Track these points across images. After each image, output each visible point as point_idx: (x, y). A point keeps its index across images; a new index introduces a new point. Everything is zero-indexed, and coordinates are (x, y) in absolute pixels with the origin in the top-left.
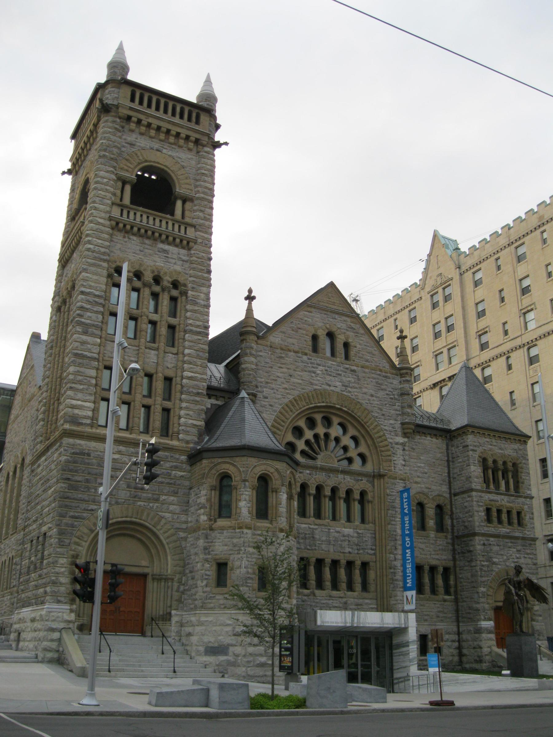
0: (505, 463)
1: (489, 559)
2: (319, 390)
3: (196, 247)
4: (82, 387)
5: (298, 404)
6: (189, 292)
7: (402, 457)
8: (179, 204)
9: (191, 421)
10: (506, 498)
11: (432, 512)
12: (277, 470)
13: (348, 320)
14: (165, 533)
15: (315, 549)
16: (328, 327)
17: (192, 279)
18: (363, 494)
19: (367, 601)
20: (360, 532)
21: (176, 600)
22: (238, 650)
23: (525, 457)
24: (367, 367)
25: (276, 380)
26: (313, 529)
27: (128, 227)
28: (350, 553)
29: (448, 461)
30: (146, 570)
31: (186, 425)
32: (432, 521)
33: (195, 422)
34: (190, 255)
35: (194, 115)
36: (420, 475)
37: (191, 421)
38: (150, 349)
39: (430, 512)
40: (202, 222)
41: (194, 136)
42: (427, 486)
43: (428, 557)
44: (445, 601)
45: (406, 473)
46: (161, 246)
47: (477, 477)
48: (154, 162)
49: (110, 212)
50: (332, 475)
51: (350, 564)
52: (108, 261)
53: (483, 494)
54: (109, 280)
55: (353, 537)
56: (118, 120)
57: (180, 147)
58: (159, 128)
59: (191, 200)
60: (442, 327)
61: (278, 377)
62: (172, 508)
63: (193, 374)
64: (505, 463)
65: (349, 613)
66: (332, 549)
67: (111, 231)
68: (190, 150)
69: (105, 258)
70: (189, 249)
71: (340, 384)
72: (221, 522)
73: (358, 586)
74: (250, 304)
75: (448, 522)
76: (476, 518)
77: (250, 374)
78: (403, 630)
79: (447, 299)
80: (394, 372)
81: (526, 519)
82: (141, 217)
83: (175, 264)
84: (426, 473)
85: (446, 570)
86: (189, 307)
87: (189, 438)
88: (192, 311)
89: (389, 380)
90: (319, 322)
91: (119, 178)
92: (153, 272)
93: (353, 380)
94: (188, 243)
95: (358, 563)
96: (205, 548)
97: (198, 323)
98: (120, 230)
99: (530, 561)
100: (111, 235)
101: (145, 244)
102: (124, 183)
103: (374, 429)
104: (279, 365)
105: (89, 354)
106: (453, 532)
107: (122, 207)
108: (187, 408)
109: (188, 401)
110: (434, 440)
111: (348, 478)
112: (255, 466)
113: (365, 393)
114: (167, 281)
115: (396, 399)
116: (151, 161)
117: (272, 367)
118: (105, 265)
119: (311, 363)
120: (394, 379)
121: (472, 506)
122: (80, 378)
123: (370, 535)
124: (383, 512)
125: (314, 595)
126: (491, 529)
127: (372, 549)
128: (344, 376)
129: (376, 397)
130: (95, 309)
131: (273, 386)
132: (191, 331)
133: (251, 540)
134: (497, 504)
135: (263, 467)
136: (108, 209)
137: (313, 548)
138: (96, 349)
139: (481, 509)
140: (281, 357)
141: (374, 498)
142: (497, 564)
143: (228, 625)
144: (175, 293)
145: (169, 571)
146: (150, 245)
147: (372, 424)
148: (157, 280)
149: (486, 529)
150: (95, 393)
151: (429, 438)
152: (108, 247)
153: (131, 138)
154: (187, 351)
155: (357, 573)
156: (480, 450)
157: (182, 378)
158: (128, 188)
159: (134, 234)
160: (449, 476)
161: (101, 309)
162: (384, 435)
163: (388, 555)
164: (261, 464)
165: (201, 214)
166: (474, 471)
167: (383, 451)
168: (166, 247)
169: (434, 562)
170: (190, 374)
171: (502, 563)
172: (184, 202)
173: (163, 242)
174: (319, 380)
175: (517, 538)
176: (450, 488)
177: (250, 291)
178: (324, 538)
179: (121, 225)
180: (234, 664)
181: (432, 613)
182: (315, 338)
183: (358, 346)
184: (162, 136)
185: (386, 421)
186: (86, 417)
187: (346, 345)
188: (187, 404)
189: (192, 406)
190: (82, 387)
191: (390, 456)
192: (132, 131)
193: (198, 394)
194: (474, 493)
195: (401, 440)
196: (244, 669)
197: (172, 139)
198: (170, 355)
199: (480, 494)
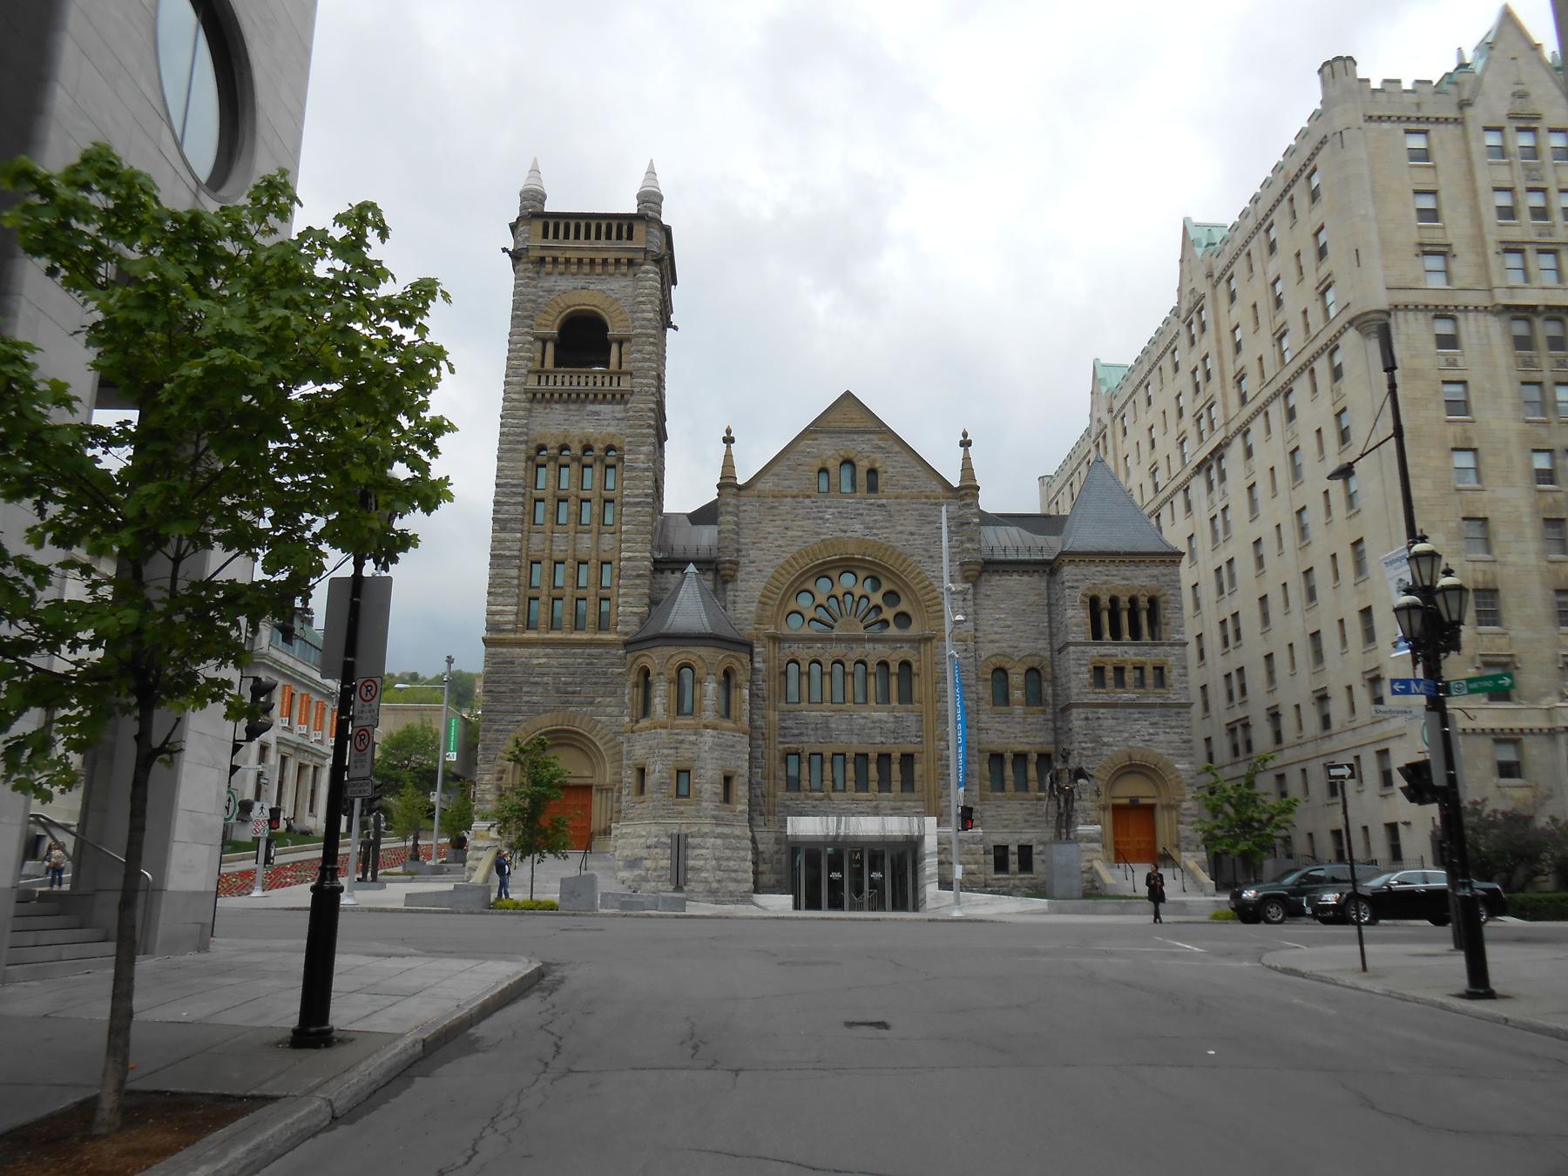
0: (1133, 601)
1: (1096, 740)
10: (1132, 650)
18: (906, 665)
22: (648, 863)
23: (1175, 585)
24: (905, 497)
27: (548, 396)
29: (1049, 605)
30: (589, 781)
34: (626, 411)
35: (625, 228)
39: (1016, 679)
41: (624, 256)
44: (1039, 799)
46: (591, 408)
47: (1077, 625)
51: (884, 758)
52: (526, 442)
53: (1088, 648)
57: (611, 275)
58: (580, 261)
59: (628, 340)
60: (1200, 376)
62: (609, 710)
64: (1133, 601)
65: (833, 820)
66: (855, 740)
68: (625, 275)
72: (644, 723)
73: (896, 786)
74: (729, 447)
75: (1048, 690)
76: (1073, 684)
78: (921, 838)
79: (1203, 328)
81: (1172, 675)
82: (567, 380)
85: (1045, 759)
87: (628, 629)
88: (630, 479)
90: (829, 450)
91: (537, 338)
95: (896, 755)
98: (540, 402)
99: (1176, 738)
100: (530, 410)
102: (544, 342)
105: (507, 553)
106: (1055, 705)
107: (539, 373)
108: (625, 595)
110: (1026, 578)
111: (879, 647)
114: (598, 447)
118: (523, 447)
126: (1102, 696)
138: (517, 546)
148: (587, 448)
151: (1015, 577)
152: (526, 425)
153: (548, 283)
155: (895, 768)
156: (1084, 586)
158: (550, 347)
160: (1050, 627)
165: (638, 356)
168: (596, 408)
169: (1019, 748)
172: (621, 344)
173: (592, 402)
175: (1152, 706)
176: (1051, 644)
179: (539, 396)
180: (645, 879)
184: (586, 269)
186: (507, 623)
187: (872, 472)
192: (549, 274)
193: (639, 576)
194: (1071, 648)
197: (598, 269)
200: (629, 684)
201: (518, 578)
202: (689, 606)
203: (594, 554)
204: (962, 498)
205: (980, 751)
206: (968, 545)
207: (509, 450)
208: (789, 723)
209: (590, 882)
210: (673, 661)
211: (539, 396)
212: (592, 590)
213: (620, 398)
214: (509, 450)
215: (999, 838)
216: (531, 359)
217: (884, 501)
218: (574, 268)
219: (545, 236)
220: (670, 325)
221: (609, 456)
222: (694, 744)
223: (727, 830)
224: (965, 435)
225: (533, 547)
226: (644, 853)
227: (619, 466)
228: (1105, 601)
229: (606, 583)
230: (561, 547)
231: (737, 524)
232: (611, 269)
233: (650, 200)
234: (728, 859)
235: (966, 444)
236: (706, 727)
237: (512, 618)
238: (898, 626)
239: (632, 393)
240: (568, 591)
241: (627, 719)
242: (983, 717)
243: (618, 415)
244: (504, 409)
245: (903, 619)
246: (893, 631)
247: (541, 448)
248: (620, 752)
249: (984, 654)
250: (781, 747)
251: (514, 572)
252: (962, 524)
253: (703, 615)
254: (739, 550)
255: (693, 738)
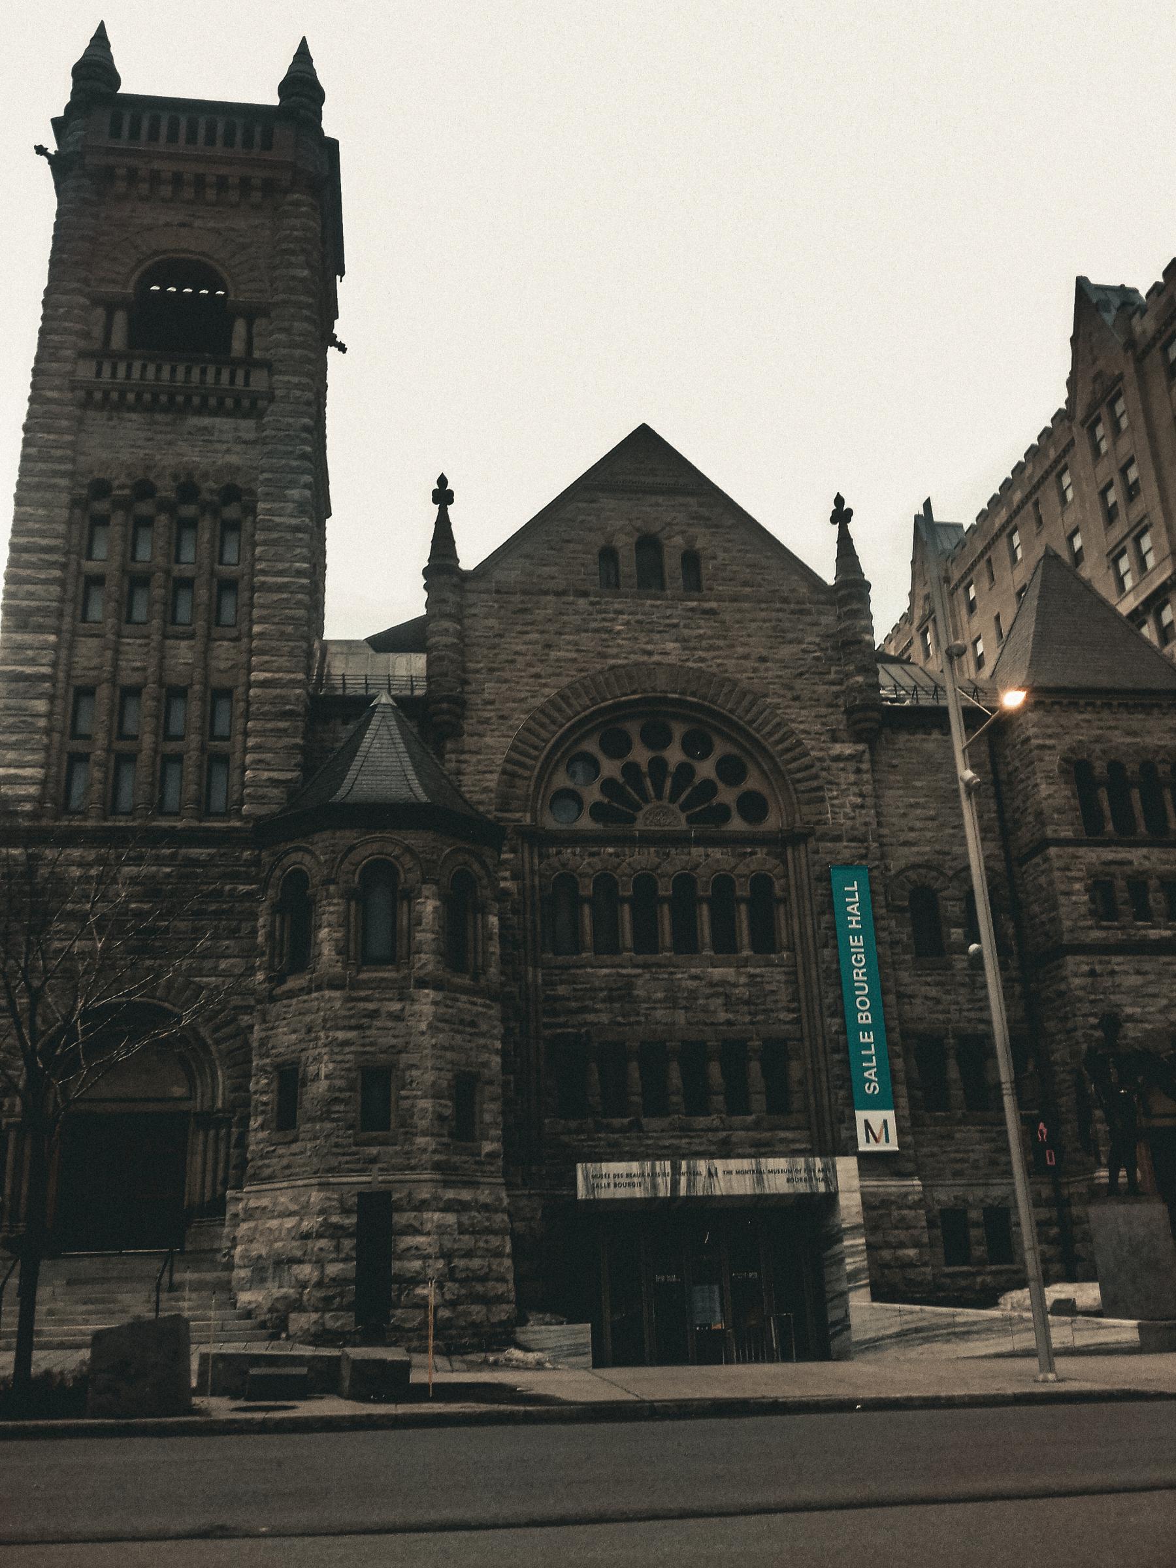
2: (624, 666)
3: (272, 407)
4: (14, 738)
5: (570, 705)
6: (261, 505)
7: (855, 789)
8: (240, 327)
9: (266, 775)
10: (1156, 853)
11: (956, 909)
12: (408, 850)
13: (691, 500)
14: (210, 1019)
15: (638, 1023)
16: (639, 523)
17: (266, 475)
18: (761, 882)
19: (782, 1134)
20: (752, 970)
21: (235, 1167)
24: (746, 598)
25: (513, 661)
26: (629, 976)
27: (114, 396)
28: (729, 1023)
31: (255, 783)
32: (960, 931)
33: (275, 775)
36: (918, 824)
37: (266, 775)
38: (177, 638)
40: (286, 351)
42: (938, 847)
43: (954, 1016)
45: (866, 824)
46: (194, 421)
47: (1059, 811)
48: (176, 251)
49: (73, 373)
50: (673, 851)
53: (1081, 851)
54: (77, 511)
55: (735, 985)
56: (86, 182)
58: (177, 180)
61: (516, 653)
63: (268, 675)
67: (78, 412)
69: (63, 467)
70: (261, 415)
71: (677, 645)
73: (758, 1101)
77: (441, 659)
78: (831, 1198)
80: (823, 597)
83: (228, 451)
84: (933, 819)
86: (260, 536)
88: (265, 543)
89: (808, 619)
92: (175, 477)
93: (709, 632)
94: (254, 404)
96: (263, 1042)
97: (280, 566)
101: (156, 423)
103: (770, 734)
104: (519, 628)
109: (261, 733)
111: (716, 853)
112: (352, 848)
113: (746, 657)
115: (830, 659)
116: (165, 252)
117: (501, 636)
118: (64, 482)
119: (599, 612)
120: (820, 613)
121: (1051, 883)
122: (11, 720)
123: (783, 978)
124: (809, 921)
125: (637, 1126)
127: (790, 1010)
128: (686, 626)
129: (777, 661)
130: (43, 576)
131: (507, 675)
132: (264, 587)
133: (344, 1013)
134: (1127, 869)
135: (375, 847)
136: (69, 367)
137: (632, 1019)
138: (49, 656)
139: (1077, 886)
140: (524, 611)
141: (786, 889)
142: (1142, 1021)
143: (291, 1214)
144: (231, 512)
145: (219, 1104)
146: (167, 424)
147: (766, 722)
149: (1096, 934)
150: (47, 748)
152: (72, 445)
154: (256, 629)
157: (249, 685)
158: (120, 318)
159: (132, 409)
161: (57, 573)
162: (799, 743)
163: (829, 1020)
164: (367, 842)
166: (1050, 796)
167: (799, 781)
168: (206, 421)
170: (262, 676)
171: (1158, 1016)
174: (619, 646)
176: (1005, 847)
177: (442, 481)
178: (660, 995)
180: (297, 1306)
181: (973, 1156)
182: (608, 555)
183: (721, 555)
185: (803, 712)
187: (691, 560)
188: (258, 740)
189: (271, 742)
190: (14, 738)
191: (820, 788)
194: (1053, 851)
195: (848, 749)
196: (314, 1316)
198: (225, 643)
199: (1071, 850)
200: (264, 908)
201: (49, 715)
202: (383, 764)
203: (197, 675)
204: (843, 601)
205: (905, 1035)
206: (860, 679)
207: (38, 487)
208: (561, 990)
209: (172, 1335)
210: (354, 857)
211: (98, 396)
212: (194, 739)
213: (249, 406)
214: (38, 487)
215: (944, 1195)
216: (87, 335)
217: (714, 605)
218: (166, 191)
219: (116, 132)
220: (332, 341)
221: (226, 505)
222: (398, 1017)
223: (466, 1195)
224: (839, 500)
225: (81, 662)
226: (295, 1248)
227: (248, 524)
228: (1100, 767)
229: (221, 727)
230: (136, 660)
231: (461, 636)
232: (234, 196)
233: (302, 85)
234: (469, 1254)
235: (841, 515)
236: (422, 984)
237: (33, 790)
238: (745, 817)
239: (271, 399)
240: (148, 740)
241: (260, 976)
242: (905, 976)
243: (252, 436)
244: (31, 415)
245: (753, 807)
246: (737, 824)
247: (101, 489)
248: (246, 1044)
249: (894, 866)
250: (547, 1032)
251: (41, 706)
252: (846, 644)
253: (412, 776)
254: (465, 682)
255: (396, 1006)
